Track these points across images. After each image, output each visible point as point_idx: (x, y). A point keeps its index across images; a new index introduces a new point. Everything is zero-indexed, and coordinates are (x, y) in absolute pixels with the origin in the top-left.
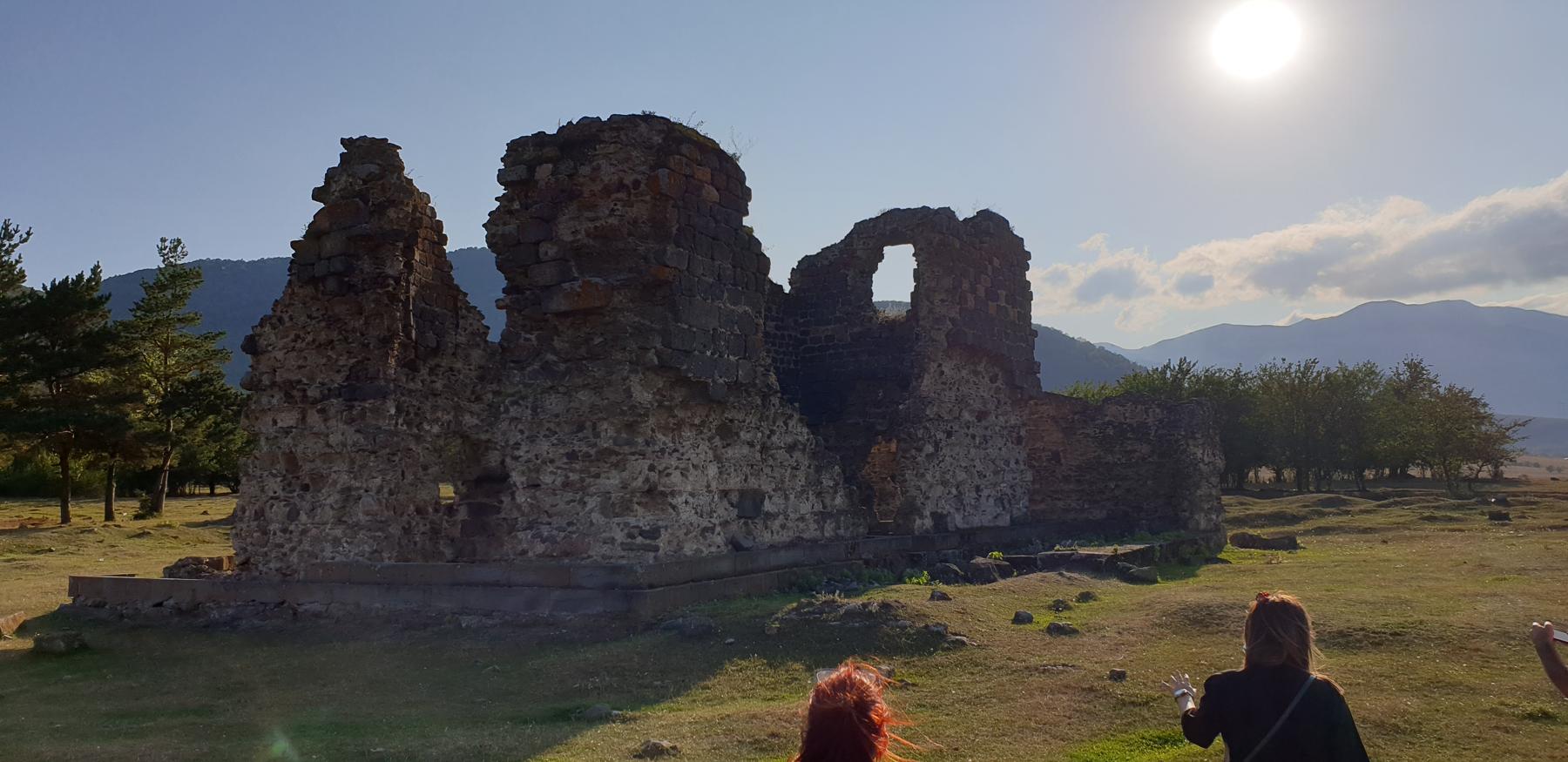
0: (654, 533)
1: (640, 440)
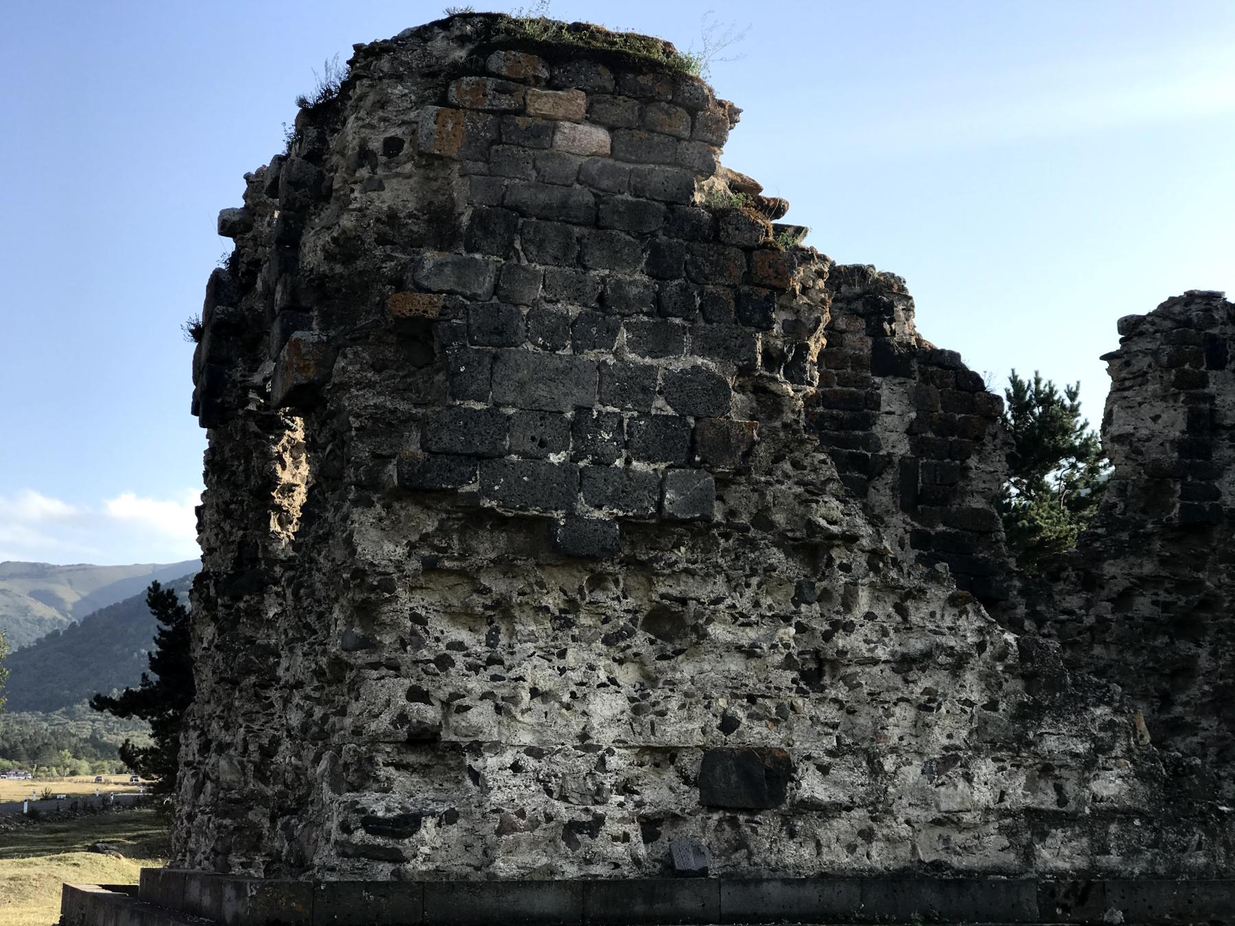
0: (408, 823)
1: (387, 639)
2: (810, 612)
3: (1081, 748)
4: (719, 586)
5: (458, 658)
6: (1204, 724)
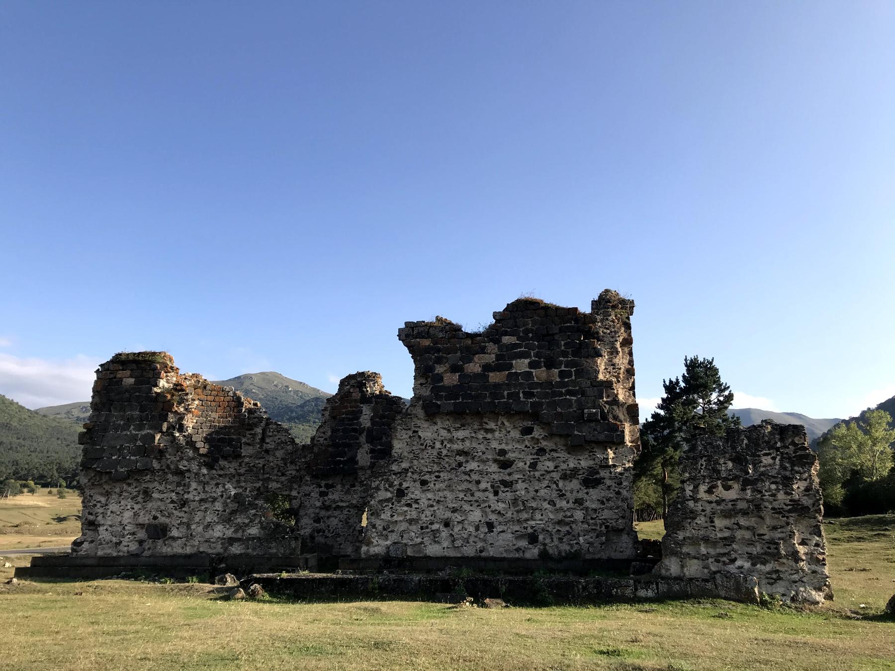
2: (179, 489)
3: (247, 521)
4: (156, 484)
5: (99, 505)
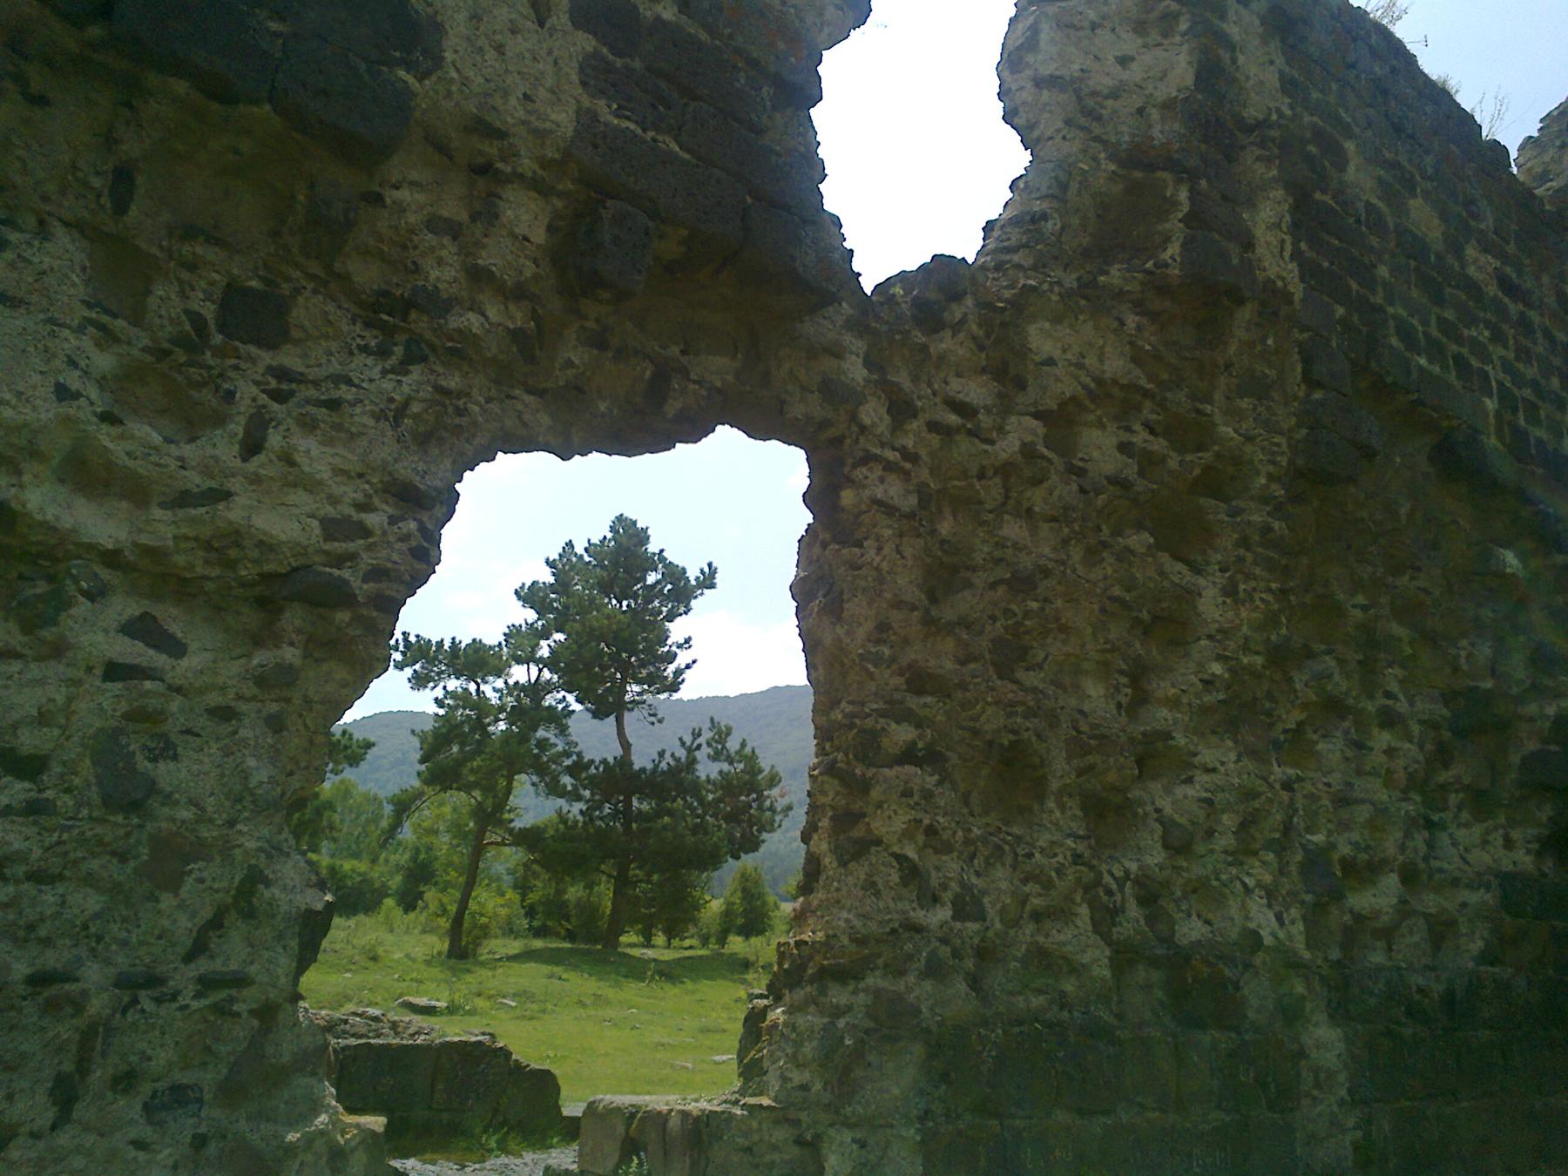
6: (1207, 756)
